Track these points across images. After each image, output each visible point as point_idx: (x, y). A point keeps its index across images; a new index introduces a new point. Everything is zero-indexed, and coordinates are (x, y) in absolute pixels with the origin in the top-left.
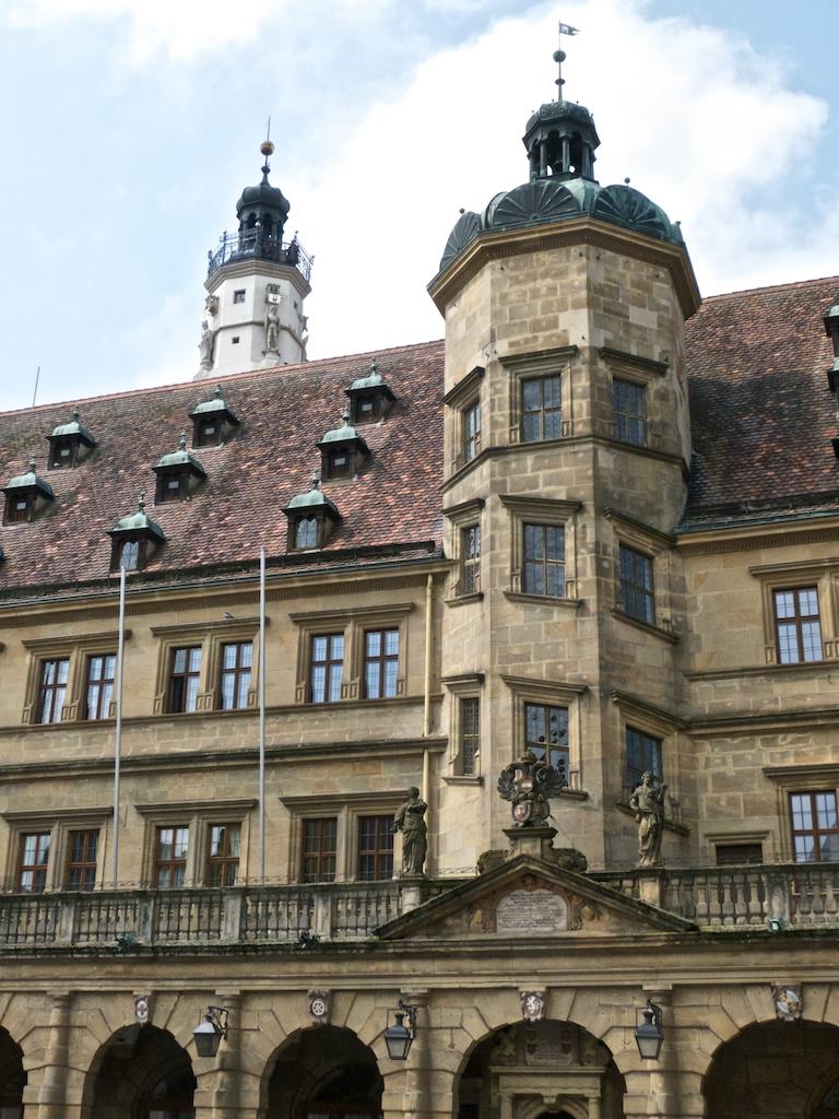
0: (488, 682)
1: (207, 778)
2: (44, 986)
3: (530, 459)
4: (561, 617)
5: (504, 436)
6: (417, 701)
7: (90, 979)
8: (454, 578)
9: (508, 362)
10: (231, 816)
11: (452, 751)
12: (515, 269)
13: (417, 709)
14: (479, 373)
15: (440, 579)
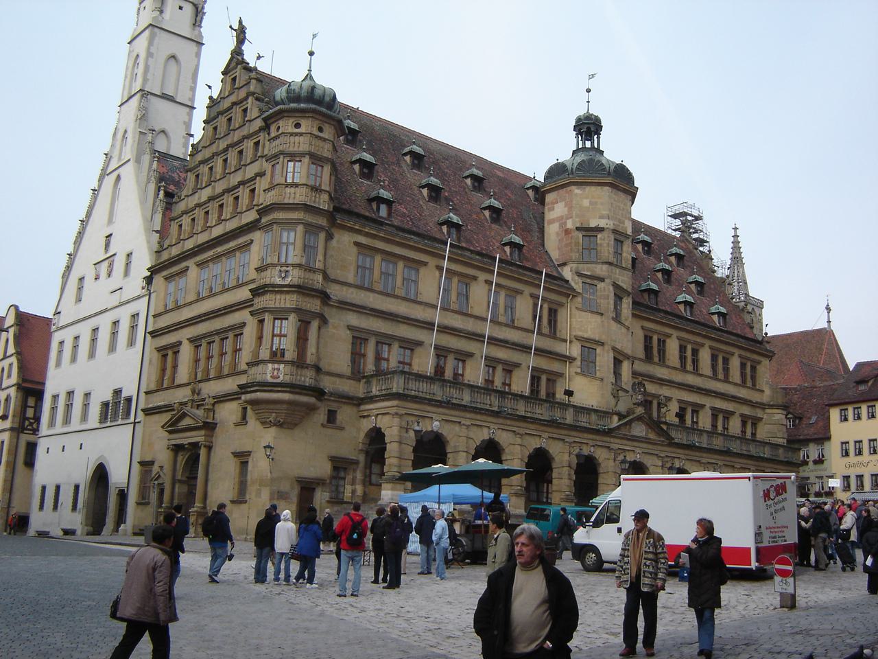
0: (606, 347)
1: (504, 349)
2: (514, 429)
3: (618, 271)
4: (624, 330)
5: (611, 259)
6: (565, 341)
7: (531, 428)
8: (579, 299)
9: (615, 231)
10: (510, 368)
11: (578, 363)
12: (615, 194)
13: (564, 344)
14: (601, 230)
15: (574, 296)
